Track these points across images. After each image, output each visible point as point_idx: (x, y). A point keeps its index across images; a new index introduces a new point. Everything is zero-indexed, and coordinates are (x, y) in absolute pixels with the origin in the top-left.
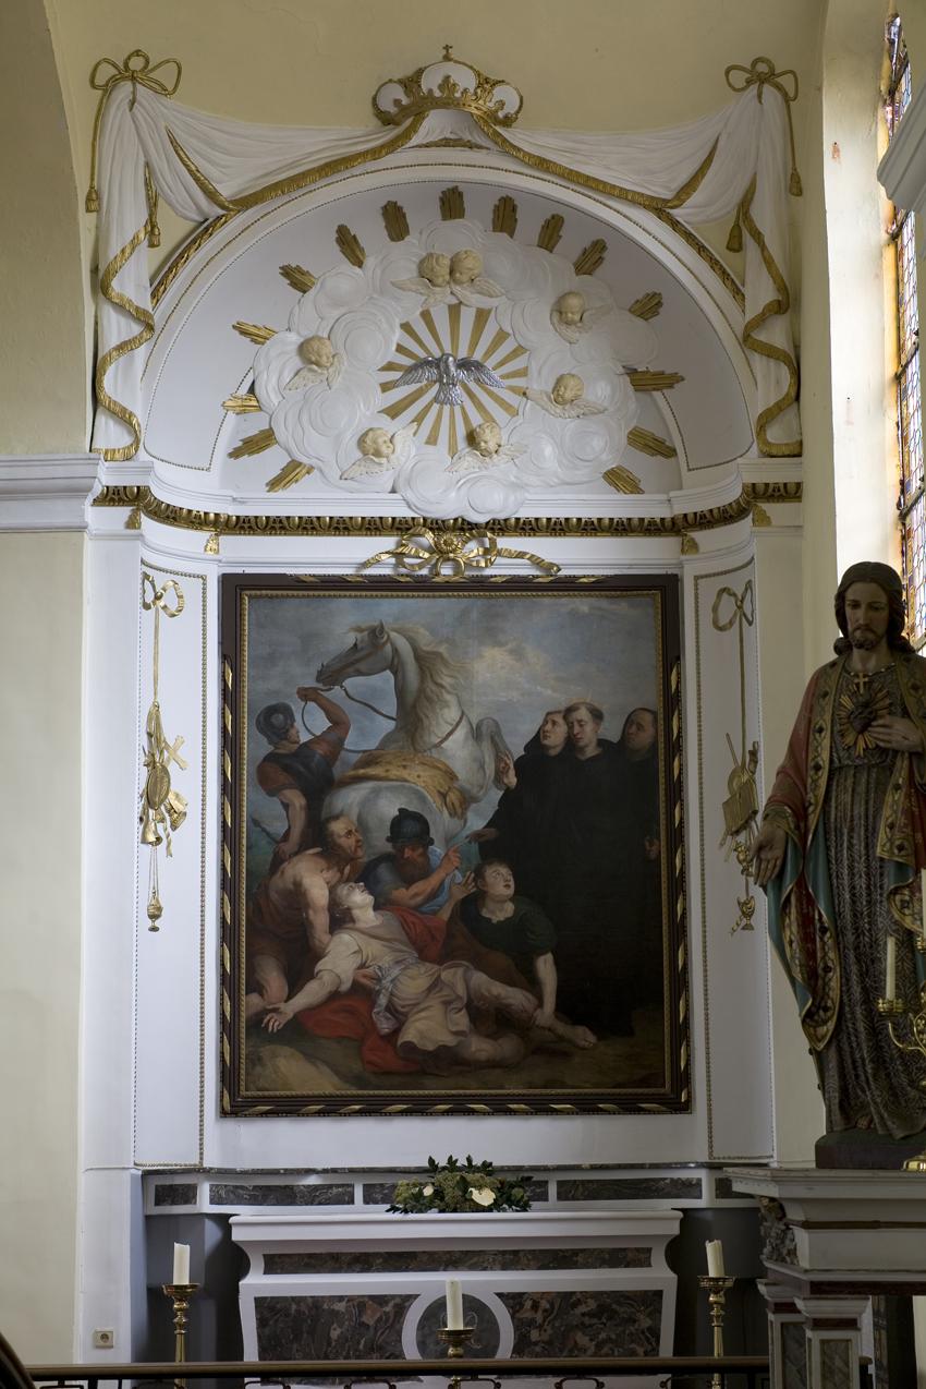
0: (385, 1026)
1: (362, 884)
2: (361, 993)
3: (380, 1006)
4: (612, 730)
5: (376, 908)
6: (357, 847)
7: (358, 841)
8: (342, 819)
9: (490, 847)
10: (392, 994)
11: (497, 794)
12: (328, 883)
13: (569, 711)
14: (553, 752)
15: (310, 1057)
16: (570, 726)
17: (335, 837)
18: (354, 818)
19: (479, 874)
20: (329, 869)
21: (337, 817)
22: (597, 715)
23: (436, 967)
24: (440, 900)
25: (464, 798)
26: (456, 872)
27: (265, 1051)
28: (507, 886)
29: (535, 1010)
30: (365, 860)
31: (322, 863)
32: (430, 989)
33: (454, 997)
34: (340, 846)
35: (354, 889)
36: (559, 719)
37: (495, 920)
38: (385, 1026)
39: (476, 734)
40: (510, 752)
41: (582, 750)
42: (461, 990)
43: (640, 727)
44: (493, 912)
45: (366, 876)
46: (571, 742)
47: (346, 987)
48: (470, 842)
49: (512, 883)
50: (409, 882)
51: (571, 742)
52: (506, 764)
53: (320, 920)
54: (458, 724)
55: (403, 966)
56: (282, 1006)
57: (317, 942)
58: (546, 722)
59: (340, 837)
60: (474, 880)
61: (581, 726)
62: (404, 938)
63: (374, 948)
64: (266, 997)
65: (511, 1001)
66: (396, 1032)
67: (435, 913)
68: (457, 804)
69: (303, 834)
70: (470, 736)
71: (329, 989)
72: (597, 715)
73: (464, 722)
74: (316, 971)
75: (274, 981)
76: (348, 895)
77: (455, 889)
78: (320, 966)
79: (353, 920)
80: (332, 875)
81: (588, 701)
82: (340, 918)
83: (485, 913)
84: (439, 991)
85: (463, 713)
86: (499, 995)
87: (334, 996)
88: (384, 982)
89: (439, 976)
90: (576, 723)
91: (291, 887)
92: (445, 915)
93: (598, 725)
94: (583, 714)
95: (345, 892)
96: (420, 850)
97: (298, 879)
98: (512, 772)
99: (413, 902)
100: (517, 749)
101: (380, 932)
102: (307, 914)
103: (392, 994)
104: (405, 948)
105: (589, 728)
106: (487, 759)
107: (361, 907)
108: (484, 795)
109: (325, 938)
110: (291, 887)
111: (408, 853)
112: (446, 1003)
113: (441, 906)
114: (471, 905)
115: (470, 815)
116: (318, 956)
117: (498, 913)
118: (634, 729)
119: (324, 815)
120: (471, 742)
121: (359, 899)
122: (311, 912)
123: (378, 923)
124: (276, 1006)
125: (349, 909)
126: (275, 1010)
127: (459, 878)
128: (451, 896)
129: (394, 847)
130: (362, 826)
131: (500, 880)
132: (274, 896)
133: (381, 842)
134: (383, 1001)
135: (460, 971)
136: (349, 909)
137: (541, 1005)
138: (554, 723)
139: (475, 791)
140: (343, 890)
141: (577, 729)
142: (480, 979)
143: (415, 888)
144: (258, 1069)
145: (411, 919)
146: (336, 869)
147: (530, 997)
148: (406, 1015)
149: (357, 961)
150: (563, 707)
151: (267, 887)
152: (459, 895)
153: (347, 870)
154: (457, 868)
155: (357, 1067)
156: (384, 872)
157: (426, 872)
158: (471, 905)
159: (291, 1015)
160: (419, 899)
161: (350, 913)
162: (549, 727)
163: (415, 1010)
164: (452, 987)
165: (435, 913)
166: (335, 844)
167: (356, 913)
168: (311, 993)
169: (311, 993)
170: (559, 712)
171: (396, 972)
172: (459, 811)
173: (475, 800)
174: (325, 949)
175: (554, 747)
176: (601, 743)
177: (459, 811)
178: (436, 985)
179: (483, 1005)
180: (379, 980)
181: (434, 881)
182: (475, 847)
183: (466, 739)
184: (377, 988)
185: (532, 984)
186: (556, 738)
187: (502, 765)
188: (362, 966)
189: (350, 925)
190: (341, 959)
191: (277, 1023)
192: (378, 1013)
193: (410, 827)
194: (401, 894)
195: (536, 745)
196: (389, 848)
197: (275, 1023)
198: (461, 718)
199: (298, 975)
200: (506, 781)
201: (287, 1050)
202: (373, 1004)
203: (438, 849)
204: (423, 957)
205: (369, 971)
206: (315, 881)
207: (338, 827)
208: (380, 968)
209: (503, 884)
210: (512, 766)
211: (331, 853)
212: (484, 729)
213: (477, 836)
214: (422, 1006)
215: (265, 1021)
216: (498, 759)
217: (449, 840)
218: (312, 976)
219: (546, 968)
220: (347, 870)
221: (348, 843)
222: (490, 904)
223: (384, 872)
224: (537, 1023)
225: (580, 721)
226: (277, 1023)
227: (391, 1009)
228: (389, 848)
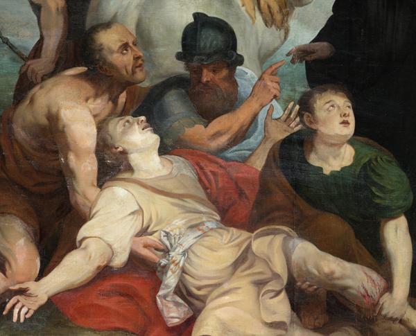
0: (174, 314)
1: (143, 118)
2: (141, 271)
3: (167, 286)
5: (163, 150)
6: (135, 67)
7: (137, 58)
8: (114, 27)
9: (322, 70)
10: (184, 271)
12: (95, 116)
17: (105, 52)
18: (132, 27)
19: (306, 106)
20: (96, 96)
21: (107, 25)
23: (245, 235)
24: (252, 141)
26: (274, 102)
28: (345, 123)
29: (381, 295)
30: (146, 84)
31: (88, 88)
32: (236, 264)
33: (268, 275)
34: (112, 66)
35: (131, 124)
37: (327, 170)
38: (174, 314)
42: (279, 266)
44: (325, 160)
45: (148, 107)
47: (120, 260)
48: (293, 62)
49: (352, 120)
50: (208, 116)
53: (84, 167)
55: (200, 233)
56: (32, 286)
57: (80, 200)
59: (112, 52)
60: (300, 114)
62: (201, 194)
63: (159, 207)
64: (9, 272)
65: (349, 282)
67: (245, 160)
68: (275, 7)
69: (62, 48)
71: (96, 264)
74: (79, 238)
76: (124, 133)
77: (273, 127)
78: (84, 232)
79: (130, 169)
80: (101, 104)
82: (112, 165)
83: (314, 160)
84: (250, 267)
86: (332, 273)
87: (104, 272)
88: (172, 254)
89: (249, 247)
91: (44, 121)
92: (259, 163)
95: (119, 129)
96: (225, 72)
97: (54, 110)
99: (214, 145)
101: (169, 186)
102: (66, 158)
103: (184, 271)
104: (202, 209)
107: (140, 151)
109: (92, 192)
110: (44, 121)
111: (207, 76)
112: (259, 284)
113: (253, 151)
114: (294, 149)
115: (293, 23)
116: (82, 219)
117: (332, 161)
119: (89, 22)
121: (139, 140)
122: (72, 157)
123: (165, 172)
124: (23, 286)
125: (124, 153)
126: (22, 292)
127: (278, 111)
128: (265, 138)
129: (188, 67)
130: (142, 38)
131: (335, 115)
132: (20, 134)
133: (169, 61)
134: (171, 280)
135: (278, 240)
136: (124, 153)
137: (389, 288)
140: (116, 127)
142: (304, 250)
143: (216, 125)
145: (209, 168)
146: (106, 97)
147: (375, 276)
148: (203, 300)
149: (134, 225)
151: (10, 121)
152: (279, 135)
153: (123, 98)
154: (275, 97)
156: (174, 103)
157: (231, 103)
158: (294, 149)
159: (43, 299)
160: (223, 140)
161: (127, 159)
163: (216, 293)
164: (267, 262)
165: (245, 160)
166: (105, 61)
167: (134, 158)
168: (72, 270)
169: (72, 270)
171: (189, 240)
172: (278, 17)
174: (91, 209)
177: (278, 17)
178: (244, 259)
179: (310, 286)
180: (166, 252)
181: (241, 116)
182: (301, 68)
184: (164, 262)
185: (378, 258)
188: (144, 232)
189: (126, 175)
190: (113, 224)
191: (24, 310)
192: (165, 297)
193: (210, 39)
194: (198, 132)
196: (179, 68)
202: (158, 284)
203: (247, 74)
204: (228, 218)
205: (152, 239)
206: (76, 112)
207: (109, 39)
208: (167, 235)
209: (338, 119)
211: (101, 76)
213: (302, 54)
214: (226, 287)
215: (8, 306)
217: (264, 57)
218: (73, 246)
219: (396, 235)
220: (123, 98)
221: (123, 61)
222: (321, 148)
223: (174, 103)
224: (384, 313)
226: (24, 310)
227: (183, 291)
228: (179, 68)
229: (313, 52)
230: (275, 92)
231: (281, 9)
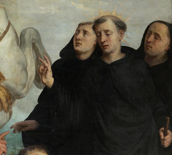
4: (133, 39)
11: (37, 92)
13: (98, 22)
14: (84, 57)
16: (99, 35)
22: (121, 27)
25: (10, 94)
36: (89, 29)
39: (20, 41)
40: (49, 58)
41: (108, 55)
43: (157, 36)
46: (99, 49)
48: (14, 132)
51: (99, 49)
52: (45, 67)
54: (5, 33)
58: (78, 31)
61: (108, 35)
70: (15, 43)
72: (121, 27)
73: (10, 31)
81: (114, 14)
85: (9, 24)
90: (103, 33)
93: (122, 34)
94: (109, 25)
98: (50, 74)
100: (55, 56)
105: (114, 36)
106: (29, 62)
108: (27, 92)
115: (14, 109)
118: (152, 38)
120: (16, 47)
138: (85, 32)
139: (19, 89)
141: (104, 38)
150: (92, 19)
162: (81, 35)
170: (89, 23)
172: (6, 105)
173: (19, 96)
175: (85, 53)
176: (125, 49)
177: (6, 105)
183: (12, 44)
186: (86, 46)
187: (42, 67)
195: (69, 51)
198: (8, 28)
200: (44, 81)
210: (50, 68)
212: (27, 37)
213: (20, 127)
216: (38, 62)
225: (106, 31)
229: (26, 126)
230: (4, 150)
231: (7, 101)
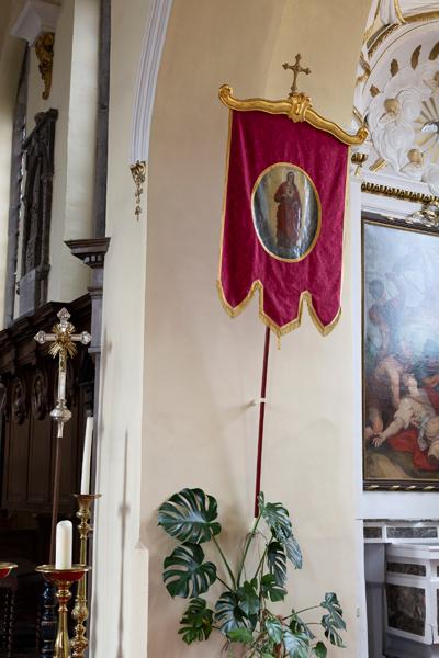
0: (423, 446)
2: (412, 430)
5: (418, 387)
15: (393, 461)
27: (374, 456)
38: (423, 446)
47: (406, 426)
53: (396, 391)
56: (381, 434)
63: (418, 407)
66: (427, 449)
75: (378, 421)
78: (396, 415)
79: (409, 392)
82: (404, 392)
87: (402, 430)
101: (420, 399)
116: (394, 409)
126: (378, 436)
134: (422, 434)
144: (371, 466)
149: (410, 413)
155: (412, 466)
167: (410, 389)
168: (393, 429)
169: (393, 429)
171: (426, 420)
180: (420, 423)
188: (413, 416)
197: (378, 443)
199: (387, 419)
201: (382, 457)
202: (418, 435)
218: (393, 420)
227: (425, 438)
